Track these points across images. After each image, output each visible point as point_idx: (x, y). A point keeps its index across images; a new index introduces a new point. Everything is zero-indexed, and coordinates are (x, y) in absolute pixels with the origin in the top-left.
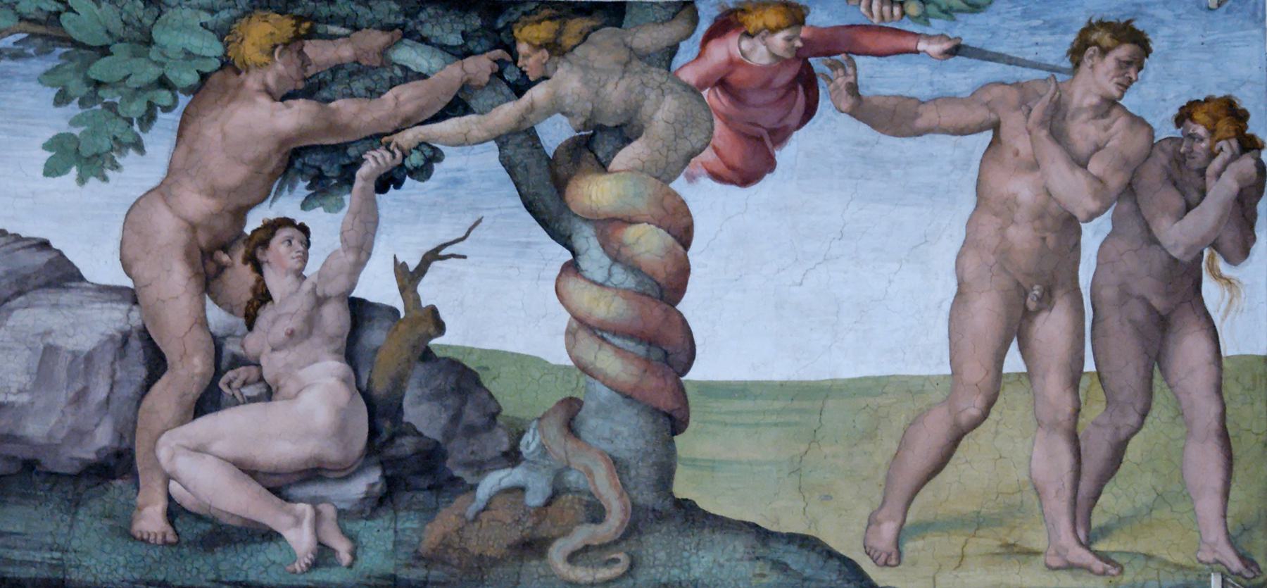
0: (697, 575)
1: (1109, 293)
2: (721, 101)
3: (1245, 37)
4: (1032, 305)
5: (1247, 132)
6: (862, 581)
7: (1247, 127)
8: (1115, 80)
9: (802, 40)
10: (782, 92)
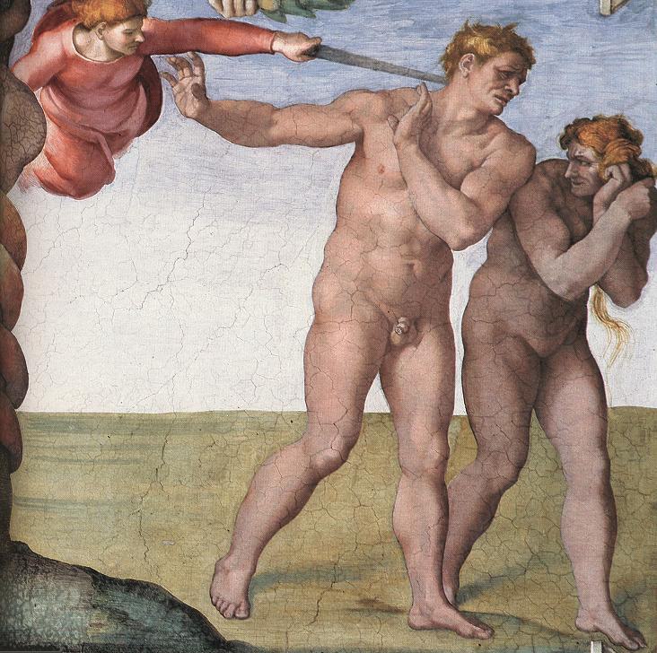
0: (30, 624)
1: (482, 331)
4: (396, 339)
5: (641, 157)
8: (494, 92)
9: (143, 34)
10: (121, 93)
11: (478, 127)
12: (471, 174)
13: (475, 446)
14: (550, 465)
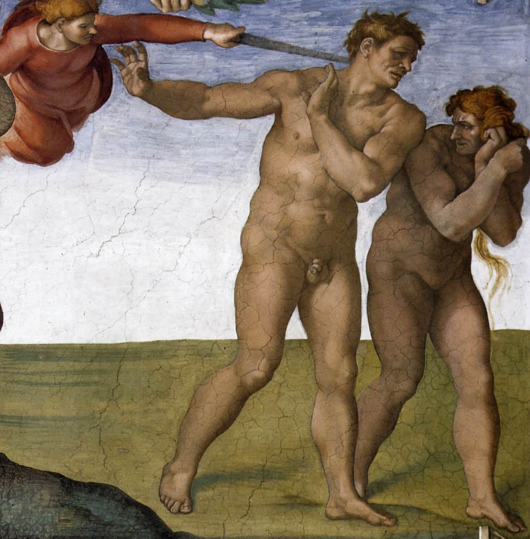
0: (8, 521)
1: (384, 269)
2: (21, 85)
3: (512, 31)
4: (312, 277)
5: (514, 121)
6: (157, 527)
7: (513, 116)
8: (390, 69)
10: (78, 76)
11: (376, 99)
12: (372, 138)
13: (380, 365)
14: (443, 380)
